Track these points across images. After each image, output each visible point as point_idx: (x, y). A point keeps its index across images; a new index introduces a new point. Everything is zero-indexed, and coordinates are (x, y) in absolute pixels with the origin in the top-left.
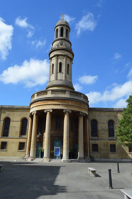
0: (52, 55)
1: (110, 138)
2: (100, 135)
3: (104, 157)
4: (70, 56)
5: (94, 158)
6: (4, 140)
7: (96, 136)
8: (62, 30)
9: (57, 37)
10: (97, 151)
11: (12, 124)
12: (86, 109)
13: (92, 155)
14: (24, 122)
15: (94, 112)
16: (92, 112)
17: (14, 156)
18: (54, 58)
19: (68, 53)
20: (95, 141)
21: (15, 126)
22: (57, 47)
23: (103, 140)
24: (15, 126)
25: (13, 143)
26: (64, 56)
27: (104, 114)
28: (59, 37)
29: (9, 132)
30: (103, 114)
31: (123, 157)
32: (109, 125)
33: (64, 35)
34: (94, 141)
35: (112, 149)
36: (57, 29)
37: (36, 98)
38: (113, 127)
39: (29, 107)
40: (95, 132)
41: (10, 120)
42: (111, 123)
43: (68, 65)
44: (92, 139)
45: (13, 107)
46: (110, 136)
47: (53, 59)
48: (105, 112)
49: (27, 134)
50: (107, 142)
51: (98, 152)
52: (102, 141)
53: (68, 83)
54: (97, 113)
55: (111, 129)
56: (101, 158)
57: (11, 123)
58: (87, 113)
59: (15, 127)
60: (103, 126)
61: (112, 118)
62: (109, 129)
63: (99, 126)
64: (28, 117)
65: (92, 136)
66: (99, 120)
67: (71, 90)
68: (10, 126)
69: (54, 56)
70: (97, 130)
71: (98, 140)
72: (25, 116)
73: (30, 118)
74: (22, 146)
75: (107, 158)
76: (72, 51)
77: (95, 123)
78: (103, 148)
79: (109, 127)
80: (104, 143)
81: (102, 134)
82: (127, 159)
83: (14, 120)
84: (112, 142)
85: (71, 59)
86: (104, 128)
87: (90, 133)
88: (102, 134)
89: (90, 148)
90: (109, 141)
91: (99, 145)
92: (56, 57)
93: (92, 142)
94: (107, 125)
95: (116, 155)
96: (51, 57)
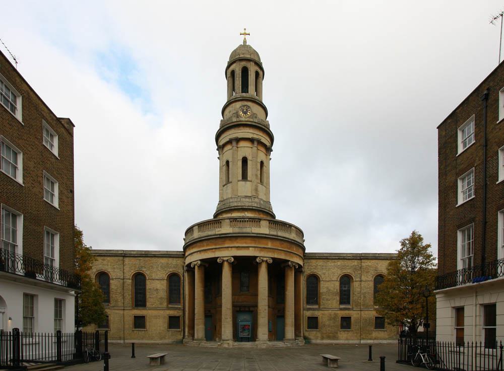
0: (224, 139)
1: (342, 306)
2: (322, 302)
3: (329, 338)
4: (265, 140)
5: (310, 339)
6: (139, 312)
7: (316, 302)
8: (245, 71)
9: (230, 93)
10: (317, 328)
11: (150, 285)
12: (300, 256)
13: (307, 334)
14: (173, 280)
15: (314, 261)
16: (309, 261)
17: (161, 339)
18: (229, 147)
19: (261, 134)
20: (313, 312)
21: (157, 287)
22: (234, 120)
23: (329, 309)
24: (157, 287)
25: (156, 317)
26: (252, 140)
27: (333, 264)
28: (238, 93)
29: (147, 300)
30: (330, 264)
31: (364, 336)
32: (341, 283)
33: (251, 88)
34: (311, 312)
35: (345, 324)
36: (233, 73)
37: (196, 234)
38: (349, 287)
39: (183, 253)
40: (313, 296)
41: (145, 277)
42: (346, 280)
43: (262, 163)
44: (309, 309)
45: (146, 253)
46: (341, 303)
47: (226, 149)
48: (336, 261)
49: (182, 301)
50: (335, 314)
51: (318, 330)
52: (326, 312)
53: (262, 202)
54: (320, 263)
55: (345, 291)
56: (322, 338)
57: (148, 282)
58: (301, 263)
59: (157, 289)
60: (329, 285)
61: (348, 271)
62: (341, 290)
63: (322, 285)
64: (180, 271)
65: (308, 303)
66: (323, 276)
67: (269, 218)
68: (148, 287)
69: (230, 142)
70: (317, 294)
71: (319, 309)
72: (174, 269)
73: (186, 275)
74: (174, 322)
75: (334, 339)
76: (269, 129)
77: (314, 280)
78: (327, 323)
79: (341, 287)
80: (330, 315)
81: (327, 300)
82: (371, 339)
83: (153, 277)
84: (345, 313)
85: (268, 150)
86: (332, 289)
87: (305, 299)
88: (327, 300)
89: (304, 324)
90: (339, 312)
91: (320, 320)
92: (234, 143)
93: (308, 314)
94: (338, 284)
95: (350, 334)
96: (221, 144)
